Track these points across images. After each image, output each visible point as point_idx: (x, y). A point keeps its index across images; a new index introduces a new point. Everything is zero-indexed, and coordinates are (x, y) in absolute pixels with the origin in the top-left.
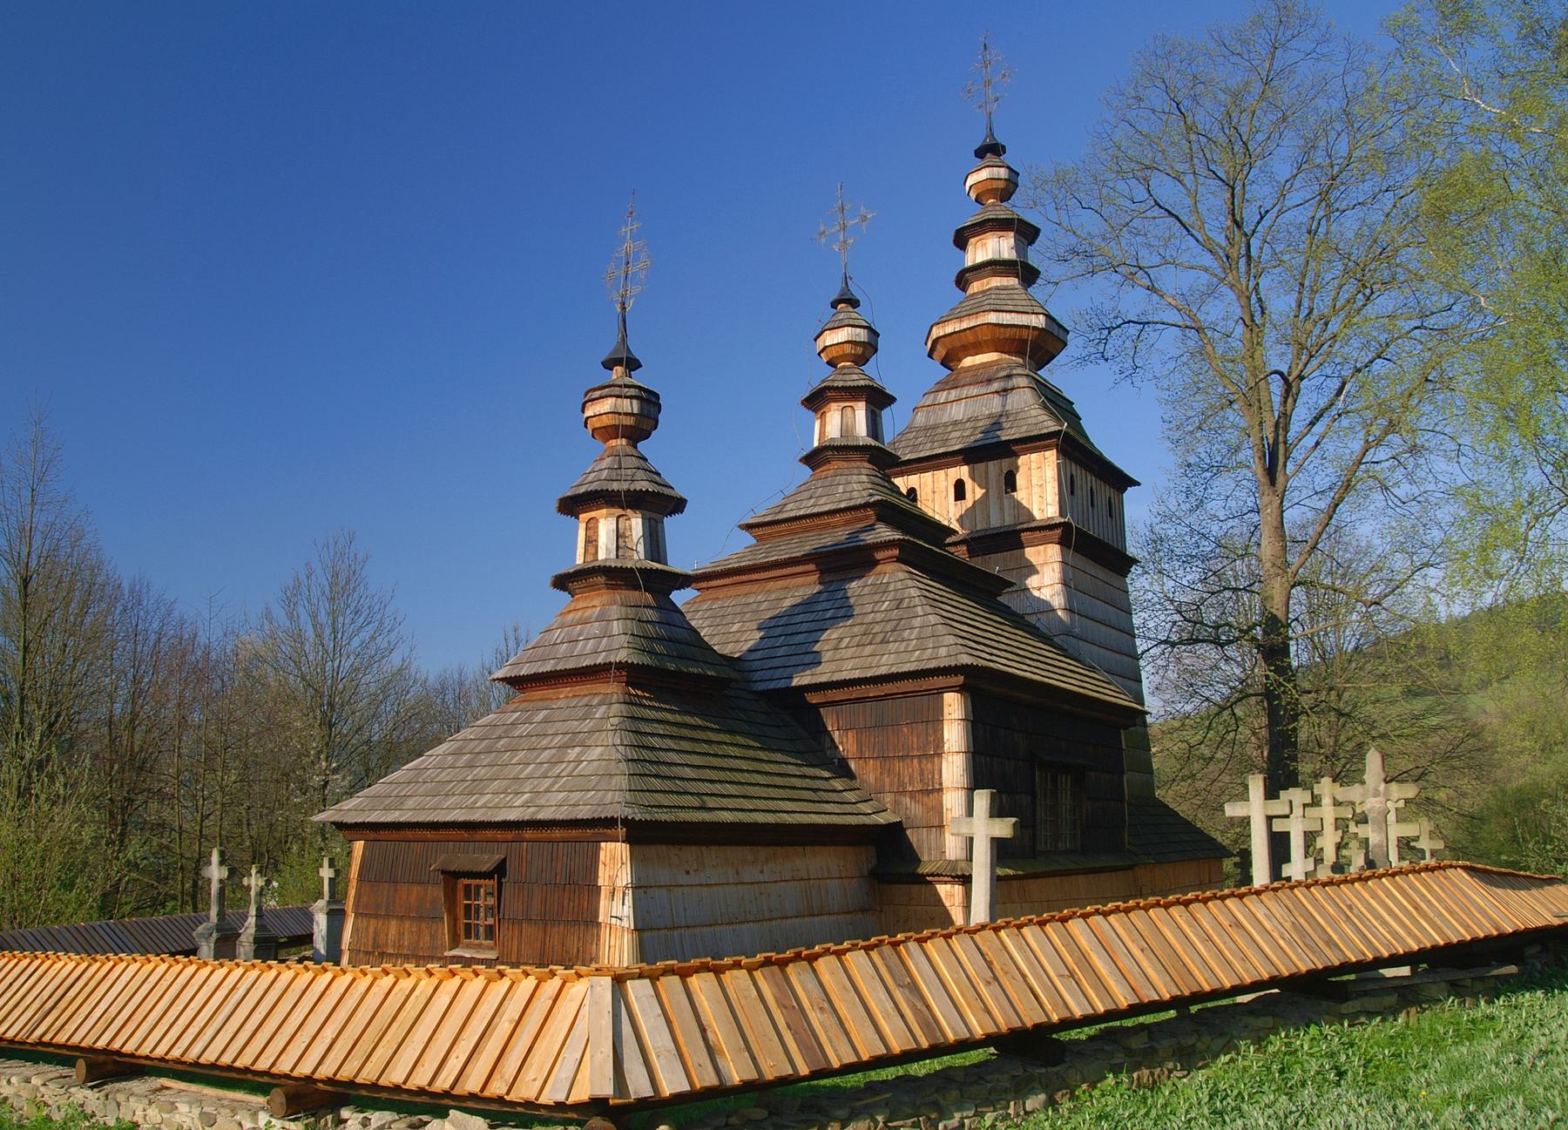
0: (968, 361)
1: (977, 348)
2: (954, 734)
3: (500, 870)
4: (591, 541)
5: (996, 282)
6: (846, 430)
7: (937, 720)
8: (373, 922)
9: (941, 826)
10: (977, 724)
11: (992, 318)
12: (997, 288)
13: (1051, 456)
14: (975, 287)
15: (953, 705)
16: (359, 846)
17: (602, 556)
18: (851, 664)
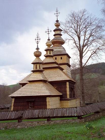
0: (55, 44)
3: (35, 101)
4: (36, 67)
5: (58, 36)
7: (66, 85)
9: (67, 95)
10: (69, 85)
13: (66, 56)
14: (56, 36)
15: (68, 83)
16: (13, 99)
17: (38, 68)
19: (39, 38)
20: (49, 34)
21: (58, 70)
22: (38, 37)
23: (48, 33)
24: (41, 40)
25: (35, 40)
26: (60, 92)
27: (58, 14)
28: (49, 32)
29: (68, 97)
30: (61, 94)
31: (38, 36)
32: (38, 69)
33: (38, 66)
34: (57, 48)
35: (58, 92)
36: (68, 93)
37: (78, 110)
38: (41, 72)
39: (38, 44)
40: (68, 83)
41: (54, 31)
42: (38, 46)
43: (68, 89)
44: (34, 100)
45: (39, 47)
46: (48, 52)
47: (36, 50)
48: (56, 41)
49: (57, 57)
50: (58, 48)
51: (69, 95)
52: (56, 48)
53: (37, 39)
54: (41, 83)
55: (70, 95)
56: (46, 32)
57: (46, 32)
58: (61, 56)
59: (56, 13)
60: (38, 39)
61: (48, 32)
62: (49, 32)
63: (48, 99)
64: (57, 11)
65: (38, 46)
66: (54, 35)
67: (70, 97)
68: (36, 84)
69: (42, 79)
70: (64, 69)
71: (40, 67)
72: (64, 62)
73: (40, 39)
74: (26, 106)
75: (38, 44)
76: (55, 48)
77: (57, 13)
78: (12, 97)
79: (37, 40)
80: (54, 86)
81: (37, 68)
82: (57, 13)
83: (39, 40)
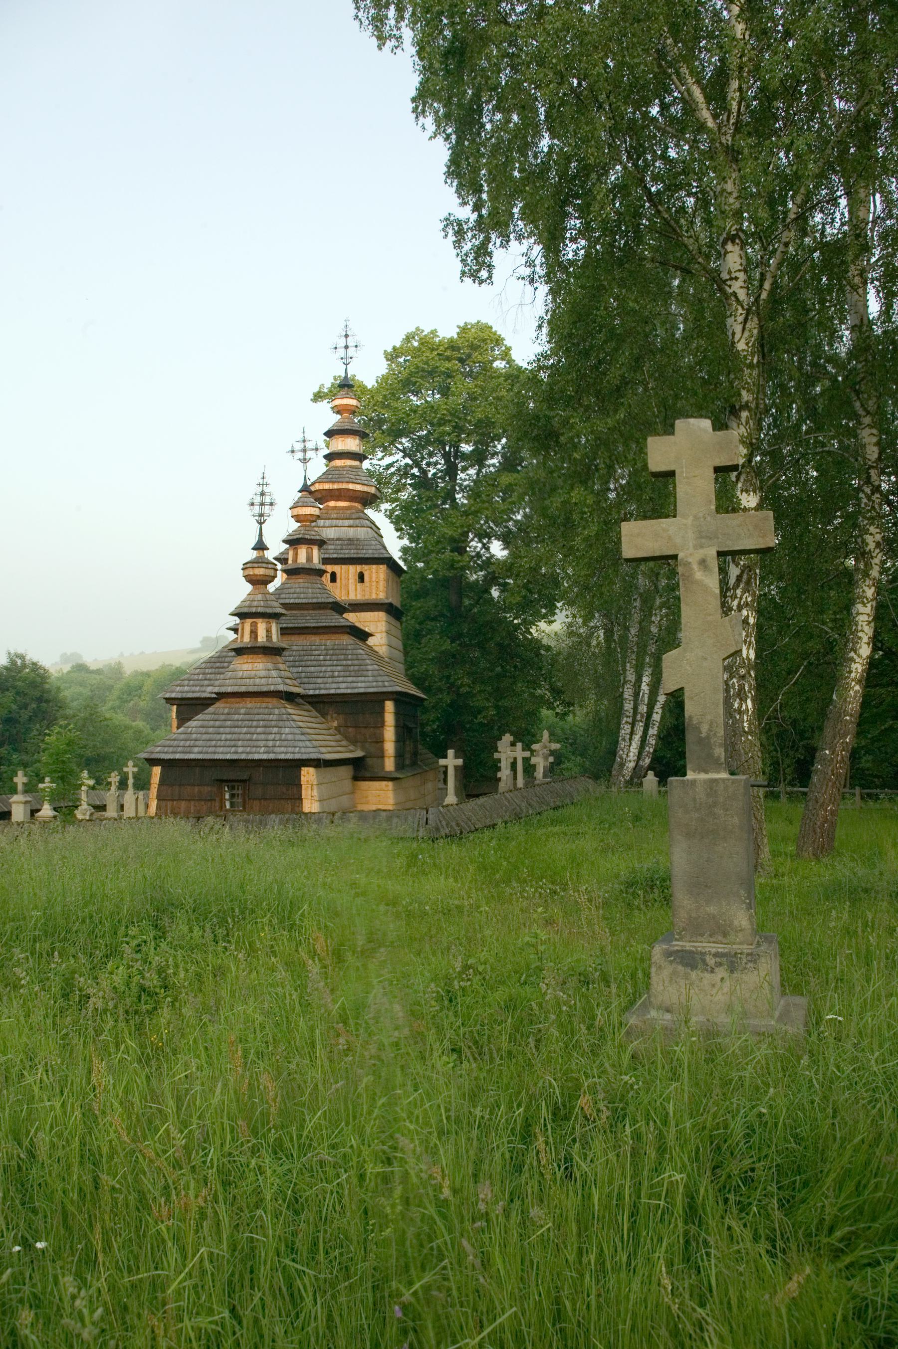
0: (332, 504)
1: (338, 499)
2: (390, 718)
4: (254, 633)
5: (349, 462)
6: (309, 559)
7: (382, 711)
8: (169, 804)
10: (397, 714)
11: (351, 486)
12: (350, 467)
13: (383, 568)
14: (338, 463)
15: (389, 706)
16: (157, 771)
17: (260, 639)
18: (343, 685)
19: (267, 500)
20: (305, 461)
21: (347, 640)
22: (263, 494)
23: (300, 455)
24: (275, 507)
25: (249, 507)
26: (354, 742)
27: (351, 352)
28: (309, 454)
29: (389, 765)
30: (359, 754)
31: (266, 490)
32: (262, 637)
33: (262, 626)
34: (340, 522)
35: (344, 743)
36: (390, 747)
37: (431, 817)
38: (275, 655)
39: (261, 523)
40: (389, 706)
41: (330, 434)
42: (261, 535)
43: (389, 733)
44: (245, 777)
45: (267, 541)
46: (302, 553)
47: (255, 554)
48: (336, 486)
49: (336, 568)
50: (347, 522)
51: (392, 759)
52: (334, 522)
53: (258, 500)
54: (274, 701)
55: (399, 756)
56: (293, 452)
57: (293, 452)
58: (359, 568)
59: (342, 342)
60: (262, 504)
61: (305, 450)
62: (309, 454)
63: (308, 775)
64: (347, 336)
65: (261, 535)
66: (329, 457)
67: (400, 766)
68: (250, 704)
69: (281, 688)
70: (371, 635)
71: (268, 631)
72: (374, 596)
73: (271, 504)
74: (211, 800)
75: (261, 523)
76: (328, 523)
77: (346, 347)
78: (153, 762)
79: (257, 509)
80: (329, 717)
81: (256, 637)
82: (346, 347)
83: (267, 509)
